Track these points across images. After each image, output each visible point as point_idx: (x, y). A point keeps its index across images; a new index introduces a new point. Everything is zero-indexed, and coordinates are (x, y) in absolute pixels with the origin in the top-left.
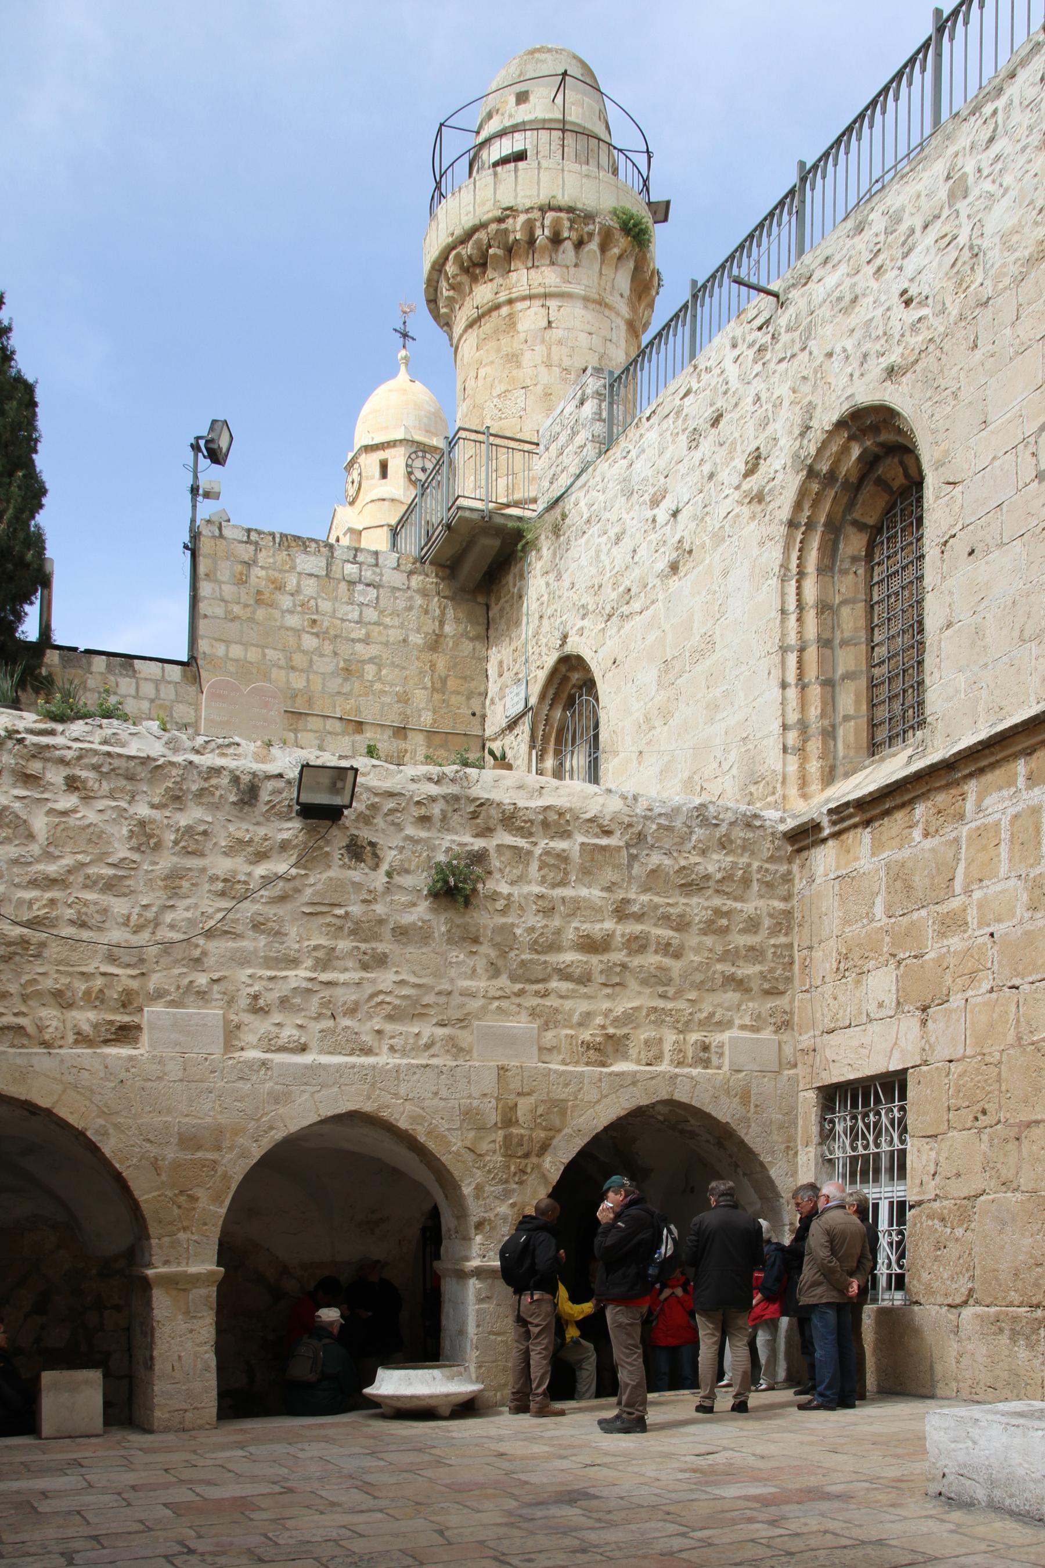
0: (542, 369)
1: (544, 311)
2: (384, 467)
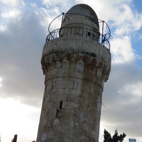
0: (49, 103)
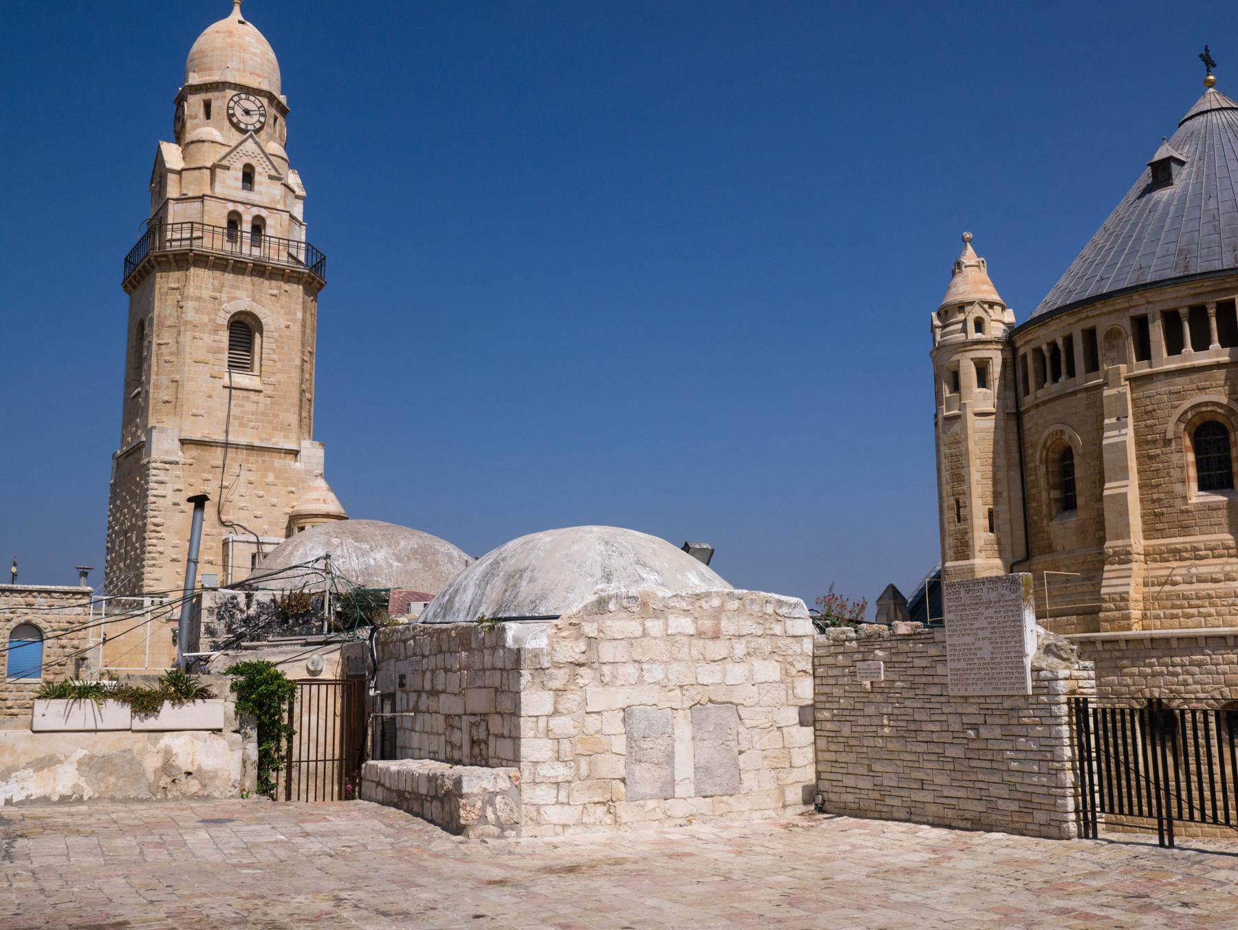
2: (207, 105)
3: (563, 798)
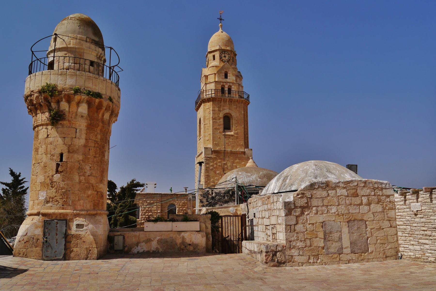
0: (44, 156)
1: (46, 130)
2: (214, 56)
3: (301, 253)
